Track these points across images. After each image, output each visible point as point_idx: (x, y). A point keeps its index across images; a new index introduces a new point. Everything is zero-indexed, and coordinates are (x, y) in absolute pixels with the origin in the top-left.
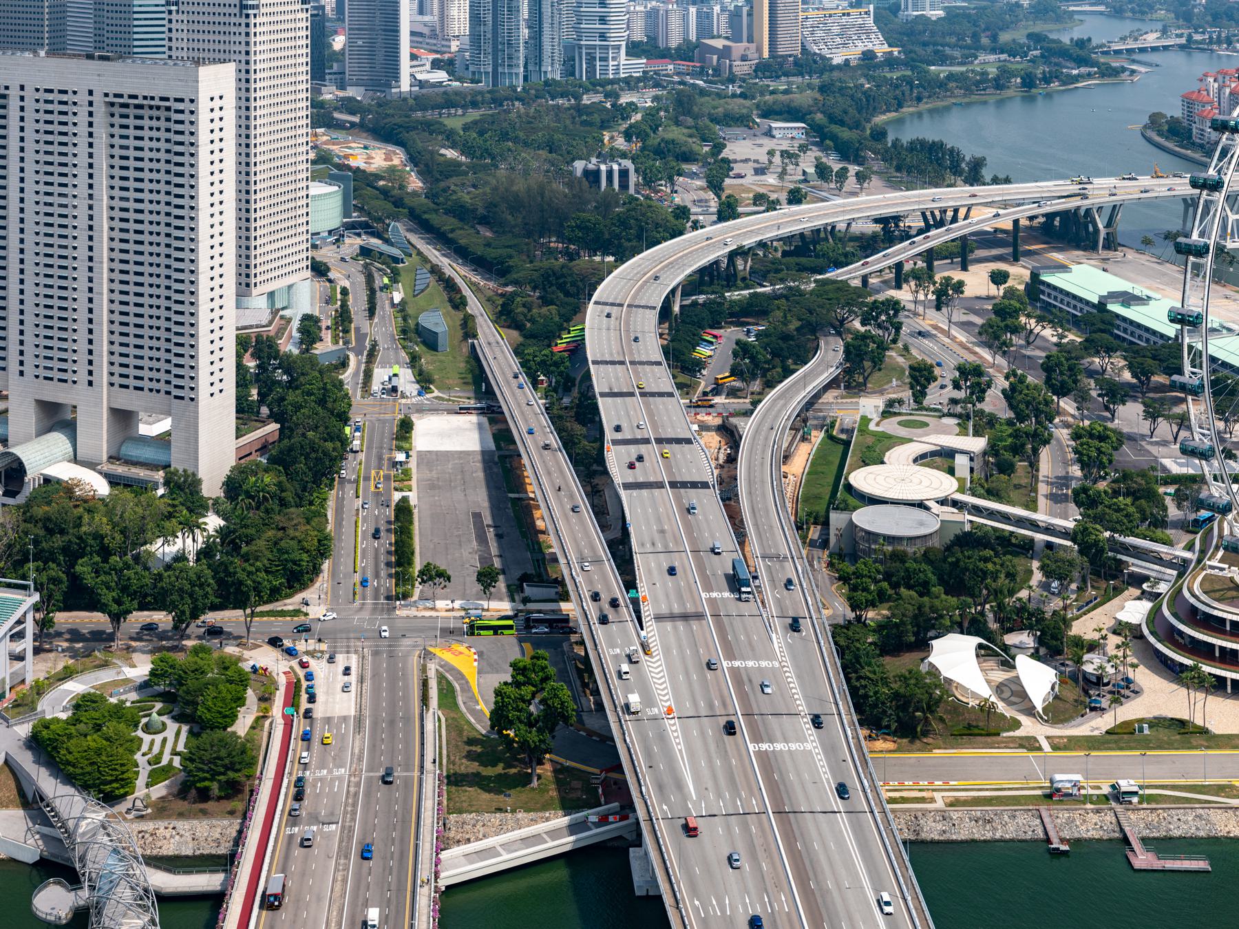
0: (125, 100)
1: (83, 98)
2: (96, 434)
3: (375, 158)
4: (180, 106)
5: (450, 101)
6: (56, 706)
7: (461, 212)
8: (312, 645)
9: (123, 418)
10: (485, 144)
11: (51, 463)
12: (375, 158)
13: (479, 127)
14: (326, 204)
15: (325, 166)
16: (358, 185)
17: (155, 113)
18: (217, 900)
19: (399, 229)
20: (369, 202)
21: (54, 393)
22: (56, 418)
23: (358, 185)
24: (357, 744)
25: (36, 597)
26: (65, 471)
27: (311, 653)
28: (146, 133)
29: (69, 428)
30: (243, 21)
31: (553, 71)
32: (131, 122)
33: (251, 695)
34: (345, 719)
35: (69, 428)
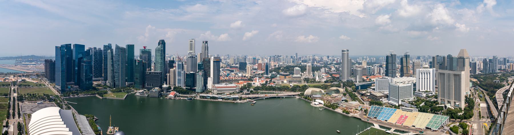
2: (453, 104)
3: (475, 80)
5: (481, 75)
7: (483, 85)
9: (455, 103)
10: (485, 79)
12: (475, 80)
13: (484, 77)
14: (471, 84)
15: (471, 81)
16: (473, 82)
19: (477, 87)
20: (474, 85)
22: (449, 102)
23: (473, 82)
26: (450, 107)
29: (450, 103)
31: (491, 72)
35: (450, 103)
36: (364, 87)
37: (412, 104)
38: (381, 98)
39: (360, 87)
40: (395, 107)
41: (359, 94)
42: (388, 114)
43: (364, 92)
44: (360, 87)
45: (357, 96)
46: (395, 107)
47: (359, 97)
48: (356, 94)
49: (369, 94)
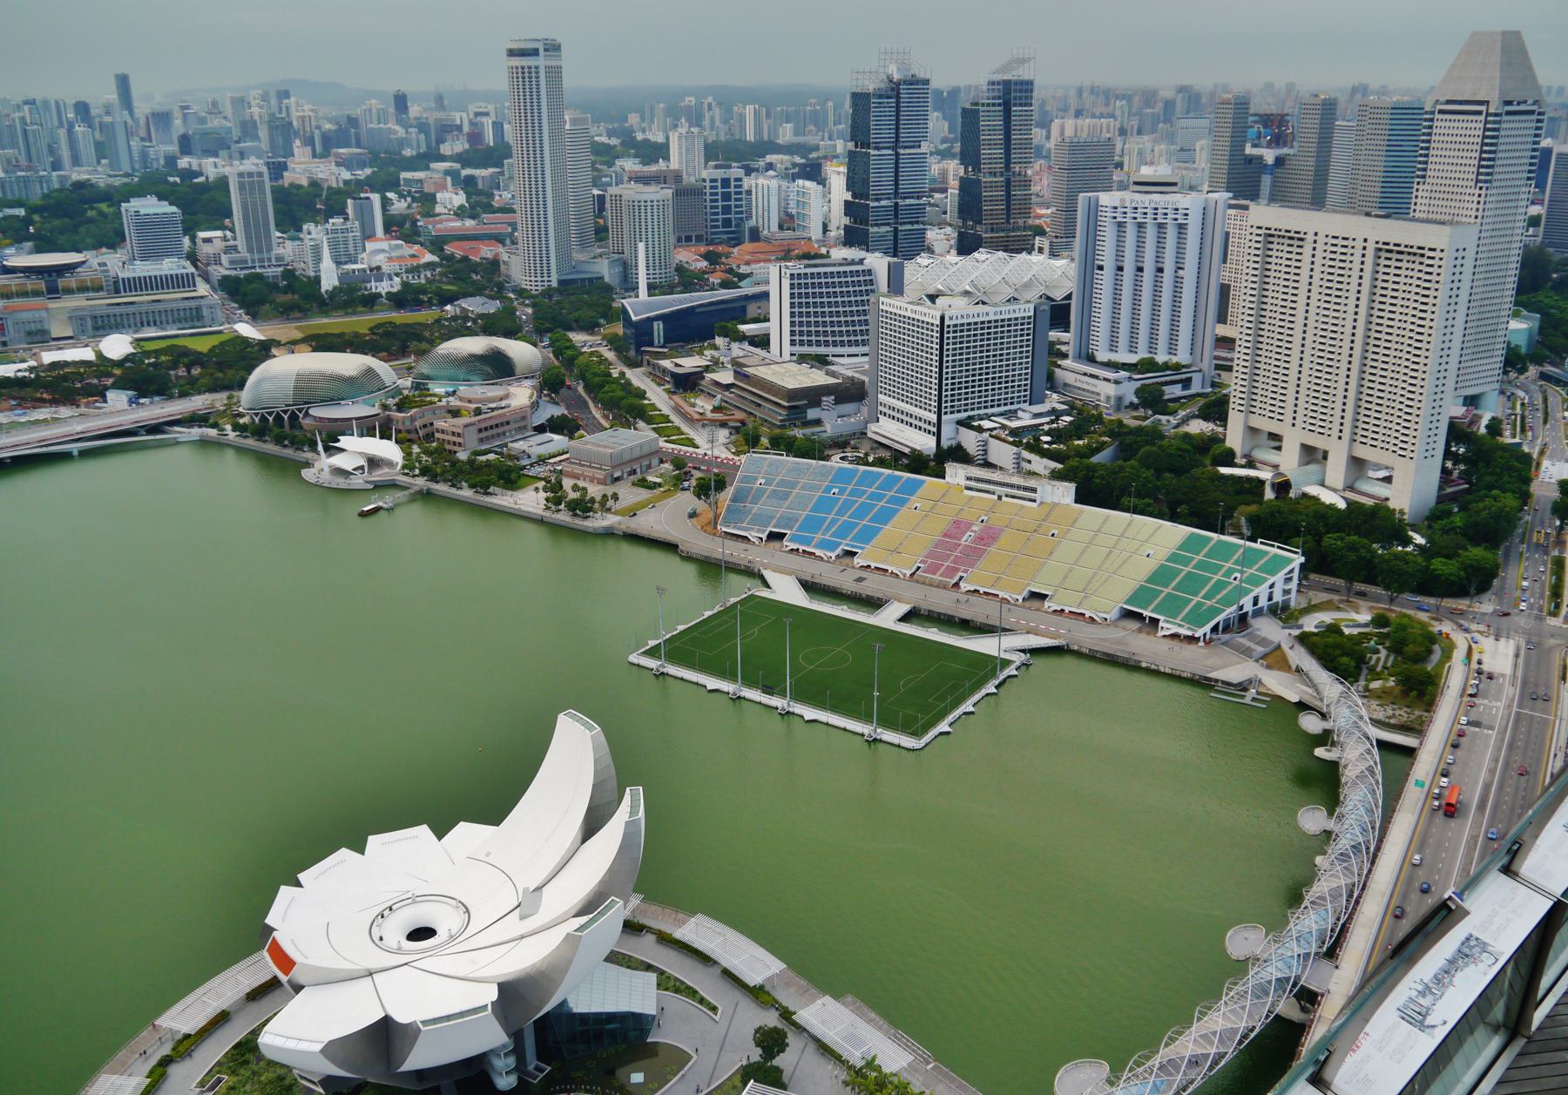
0: (1391, 247)
1: (1359, 244)
4: (1431, 254)
6: (1310, 623)
8: (1482, 628)
11: (1308, 484)
17: (1412, 258)
18: (1410, 752)
21: (1314, 440)
24: (1510, 692)
25: (1302, 559)
27: (1481, 633)
28: (1403, 272)
30: (1477, 192)
32: (1393, 263)
33: (1436, 648)
34: (1503, 675)
36: (690, 329)
37: (1035, 448)
38: (817, 403)
39: (658, 327)
40: (918, 463)
41: (658, 376)
42: (863, 511)
43: (690, 363)
44: (658, 327)
45: (641, 394)
46: (918, 463)
47: (658, 397)
48: (637, 378)
49: (726, 377)
